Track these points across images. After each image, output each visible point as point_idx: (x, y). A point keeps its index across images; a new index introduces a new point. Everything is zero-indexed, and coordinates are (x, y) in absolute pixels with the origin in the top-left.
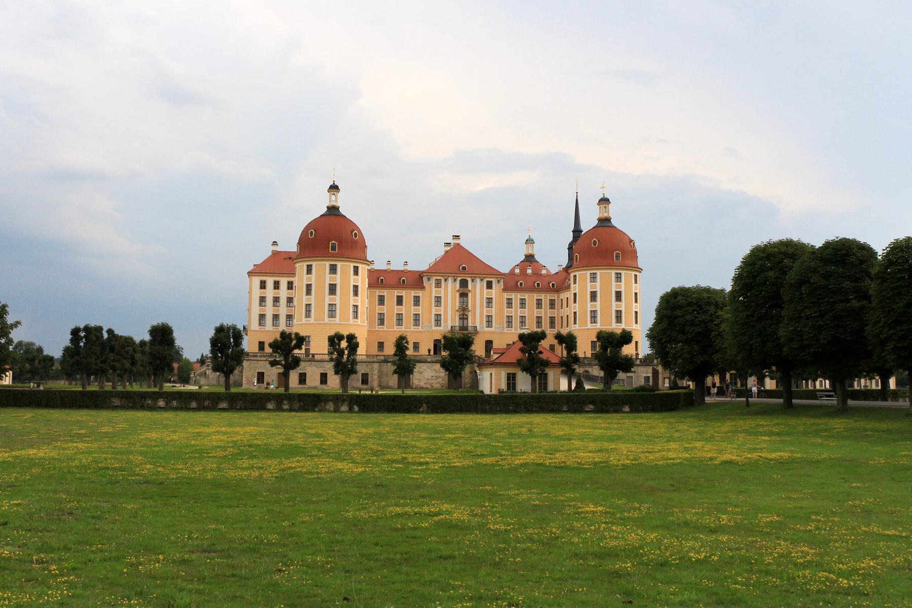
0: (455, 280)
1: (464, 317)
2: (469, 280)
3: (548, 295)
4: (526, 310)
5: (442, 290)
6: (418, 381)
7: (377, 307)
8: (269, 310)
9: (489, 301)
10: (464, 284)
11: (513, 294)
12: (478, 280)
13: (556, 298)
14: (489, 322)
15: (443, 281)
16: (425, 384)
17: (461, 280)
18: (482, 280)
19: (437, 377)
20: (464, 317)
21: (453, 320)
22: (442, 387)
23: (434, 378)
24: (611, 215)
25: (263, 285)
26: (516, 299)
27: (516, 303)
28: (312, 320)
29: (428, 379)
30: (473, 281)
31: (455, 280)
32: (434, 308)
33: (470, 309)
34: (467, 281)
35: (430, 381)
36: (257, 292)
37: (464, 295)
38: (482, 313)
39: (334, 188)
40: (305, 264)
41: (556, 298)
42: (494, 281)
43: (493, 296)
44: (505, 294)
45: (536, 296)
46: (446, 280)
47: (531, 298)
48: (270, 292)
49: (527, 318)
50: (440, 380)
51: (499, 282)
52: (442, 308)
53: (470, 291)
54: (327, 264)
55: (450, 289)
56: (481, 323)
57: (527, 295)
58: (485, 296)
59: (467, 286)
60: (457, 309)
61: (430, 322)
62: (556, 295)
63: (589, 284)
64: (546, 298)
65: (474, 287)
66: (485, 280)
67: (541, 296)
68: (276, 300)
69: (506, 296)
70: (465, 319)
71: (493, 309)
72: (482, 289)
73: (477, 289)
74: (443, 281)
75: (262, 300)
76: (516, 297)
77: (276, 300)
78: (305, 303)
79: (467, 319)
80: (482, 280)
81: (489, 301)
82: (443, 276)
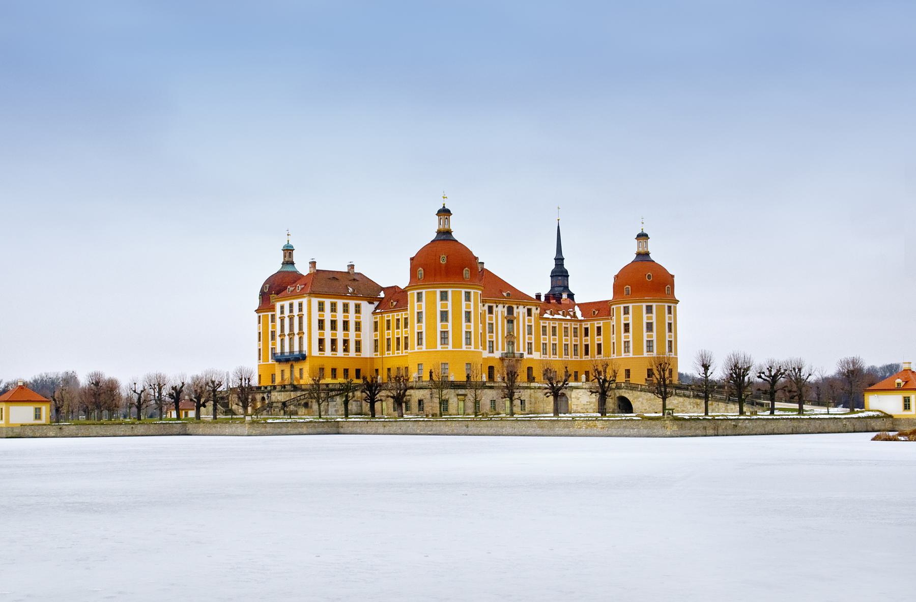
0: (504, 307)
2: (515, 307)
6: (575, 406)
8: (328, 335)
10: (510, 310)
13: (578, 326)
19: (591, 403)
23: (589, 403)
24: (650, 250)
25: (321, 307)
27: (549, 331)
29: (584, 405)
31: (504, 307)
33: (515, 335)
35: (586, 407)
37: (510, 322)
46: (497, 306)
48: (328, 316)
50: (592, 405)
51: (537, 309)
53: (515, 318)
54: (438, 291)
58: (527, 324)
59: (513, 314)
66: (526, 308)
68: (334, 324)
75: (321, 323)
77: (334, 324)
80: (524, 307)
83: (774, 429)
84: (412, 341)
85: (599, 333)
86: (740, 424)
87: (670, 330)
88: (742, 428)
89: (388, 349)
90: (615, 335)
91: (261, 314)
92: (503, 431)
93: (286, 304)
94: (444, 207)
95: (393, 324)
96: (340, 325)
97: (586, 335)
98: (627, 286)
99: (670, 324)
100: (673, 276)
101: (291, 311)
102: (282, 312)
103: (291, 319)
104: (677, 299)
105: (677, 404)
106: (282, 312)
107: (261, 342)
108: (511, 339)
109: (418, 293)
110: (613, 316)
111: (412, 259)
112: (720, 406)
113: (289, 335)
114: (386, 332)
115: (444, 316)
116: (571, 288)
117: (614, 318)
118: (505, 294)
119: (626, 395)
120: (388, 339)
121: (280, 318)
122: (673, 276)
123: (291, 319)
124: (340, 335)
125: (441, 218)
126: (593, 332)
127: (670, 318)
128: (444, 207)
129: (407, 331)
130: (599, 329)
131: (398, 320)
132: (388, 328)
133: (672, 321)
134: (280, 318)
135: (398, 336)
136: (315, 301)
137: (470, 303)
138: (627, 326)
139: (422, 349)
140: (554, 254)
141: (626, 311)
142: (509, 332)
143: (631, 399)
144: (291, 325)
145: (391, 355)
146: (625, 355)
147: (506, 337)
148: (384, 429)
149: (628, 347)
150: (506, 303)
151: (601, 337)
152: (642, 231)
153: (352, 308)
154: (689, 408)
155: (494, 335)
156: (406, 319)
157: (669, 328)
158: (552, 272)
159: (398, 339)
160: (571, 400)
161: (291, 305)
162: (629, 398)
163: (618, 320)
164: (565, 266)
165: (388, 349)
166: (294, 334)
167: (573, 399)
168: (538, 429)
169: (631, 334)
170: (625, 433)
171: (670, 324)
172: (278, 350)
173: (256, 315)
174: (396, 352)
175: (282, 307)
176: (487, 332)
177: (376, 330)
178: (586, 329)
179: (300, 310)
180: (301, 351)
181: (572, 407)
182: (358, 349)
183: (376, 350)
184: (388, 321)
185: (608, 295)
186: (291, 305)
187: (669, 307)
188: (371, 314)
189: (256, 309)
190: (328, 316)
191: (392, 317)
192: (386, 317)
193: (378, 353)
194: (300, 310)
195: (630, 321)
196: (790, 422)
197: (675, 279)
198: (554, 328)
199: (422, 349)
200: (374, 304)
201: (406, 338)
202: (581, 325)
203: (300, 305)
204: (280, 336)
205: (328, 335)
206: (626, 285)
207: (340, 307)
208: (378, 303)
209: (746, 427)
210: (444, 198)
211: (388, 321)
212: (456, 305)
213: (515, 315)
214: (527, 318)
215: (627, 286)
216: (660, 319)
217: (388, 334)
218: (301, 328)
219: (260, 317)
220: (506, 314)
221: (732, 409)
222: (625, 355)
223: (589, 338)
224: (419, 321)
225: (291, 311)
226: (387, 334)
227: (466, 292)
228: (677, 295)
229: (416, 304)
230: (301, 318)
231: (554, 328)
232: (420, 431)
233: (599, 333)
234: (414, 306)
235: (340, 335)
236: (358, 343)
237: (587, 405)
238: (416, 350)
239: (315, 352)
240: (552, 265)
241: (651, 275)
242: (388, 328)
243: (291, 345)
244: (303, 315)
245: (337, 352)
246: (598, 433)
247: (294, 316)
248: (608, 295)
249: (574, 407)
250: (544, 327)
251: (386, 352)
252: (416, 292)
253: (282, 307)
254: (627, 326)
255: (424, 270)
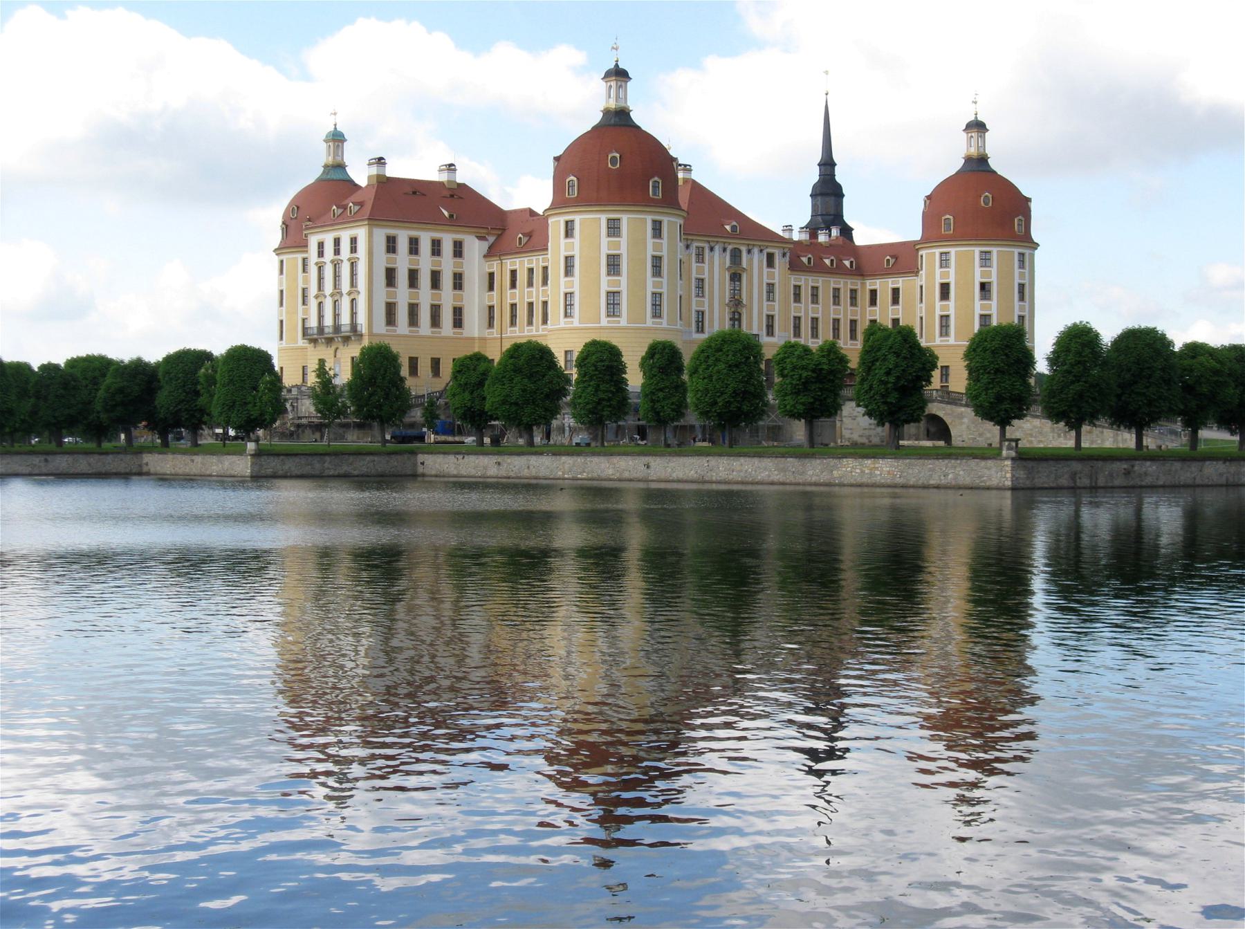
0: (725, 250)
1: (736, 318)
2: (744, 249)
3: (849, 281)
4: (820, 307)
5: (706, 266)
6: (850, 431)
7: (890, 308)
9: (771, 287)
10: (736, 255)
11: (803, 278)
12: (756, 251)
14: (770, 331)
15: (707, 251)
16: (860, 436)
17: (731, 251)
18: (761, 251)
20: (736, 318)
21: (721, 319)
22: (883, 442)
24: (989, 151)
26: (807, 285)
27: (806, 294)
28: (623, 321)
30: (749, 252)
31: (725, 250)
32: (694, 299)
33: (744, 302)
34: (740, 251)
35: (867, 432)
36: (382, 260)
37: (736, 277)
38: (760, 313)
39: (619, 75)
40: (562, 220)
41: (859, 287)
42: (777, 254)
43: (776, 281)
44: (793, 277)
45: (834, 282)
46: (712, 249)
47: (826, 284)
48: (403, 262)
49: (776, 318)
52: (706, 300)
54: (603, 218)
55: (716, 265)
56: (760, 329)
57: (821, 279)
60: (727, 301)
61: (690, 325)
62: (859, 282)
63: (978, 270)
64: (845, 285)
65: (750, 261)
66: (765, 252)
67: (840, 284)
68: (413, 276)
69: (794, 280)
70: (737, 320)
71: (776, 304)
72: (760, 268)
73: (754, 262)
74: (707, 251)
75: (390, 275)
76: (806, 282)
77: (413, 276)
78: (563, 290)
79: (739, 320)
80: (761, 251)
81: (771, 287)
82: (709, 242)
83: (1195, 478)
84: (556, 310)
85: (895, 300)
86: (1136, 468)
87: (1022, 298)
88: (1140, 475)
89: (513, 323)
90: (923, 305)
91: (284, 257)
92: (712, 476)
93: (328, 239)
94: (617, 65)
95: (522, 278)
96: (425, 280)
97: (873, 302)
98: (948, 216)
99: (1022, 287)
100: (1029, 200)
101: (337, 252)
102: (321, 254)
103: (336, 265)
104: (1035, 241)
105: (1031, 430)
106: (321, 254)
107: (284, 308)
108: (736, 306)
109: (567, 222)
110: (922, 269)
111: (557, 159)
112: (1105, 433)
113: (332, 295)
114: (509, 292)
115: (613, 265)
116: (848, 218)
117: (923, 273)
118: (728, 228)
119: (941, 414)
120: (513, 306)
121: (317, 264)
122: (1029, 200)
123: (336, 265)
124: (425, 296)
125: (611, 86)
126: (884, 297)
127: (1022, 276)
128: (617, 65)
129: (547, 290)
130: (896, 292)
131: (531, 271)
132: (513, 285)
133: (1026, 281)
134: (317, 264)
135: (530, 300)
136: (381, 234)
137: (662, 241)
138: (945, 290)
139: (572, 323)
140: (818, 156)
141: (944, 262)
142: (733, 297)
143: (948, 420)
144: (337, 276)
145: (518, 334)
146: (941, 341)
147: (727, 305)
148: (498, 470)
149: (947, 326)
150: (730, 244)
151: (900, 307)
152: (976, 118)
153: (447, 248)
154: (1051, 438)
155: (706, 300)
156: (545, 269)
157: (1019, 292)
158: (815, 187)
159: (531, 305)
160: (841, 421)
161: (337, 242)
162: (944, 419)
163: (931, 275)
164: (838, 179)
165: (513, 323)
166: (341, 294)
167: (844, 419)
168: (776, 472)
169: (951, 303)
170: (932, 482)
171: (1022, 286)
172: (313, 323)
173: (276, 260)
174: (526, 328)
175: (321, 245)
176: (693, 296)
177: (491, 288)
178: (873, 293)
179: (354, 249)
180: (354, 326)
181: (843, 434)
182: (458, 322)
183: (491, 325)
184: (513, 273)
185: (913, 232)
186: (337, 242)
187: (1022, 255)
188: (483, 260)
189: (277, 247)
190: (403, 262)
191: (521, 264)
192: (510, 263)
193: (494, 330)
194: (354, 249)
195: (952, 280)
196: (1224, 466)
197: (1033, 206)
198: (815, 289)
199: (572, 323)
200: (487, 240)
201: (545, 303)
202: (863, 285)
203: (354, 241)
204: (316, 297)
205: (403, 295)
206: (945, 214)
207: (425, 247)
208: (494, 238)
209: (1146, 474)
210: (613, 48)
211: (513, 273)
212: (637, 244)
213: (744, 264)
214: (766, 270)
215: (948, 216)
216: (1005, 275)
217: (513, 296)
218: (353, 283)
219: (282, 262)
220: (728, 263)
221: (1126, 440)
222: (941, 341)
223: (877, 309)
224: (569, 271)
225: (337, 252)
226: (510, 296)
227: (654, 222)
228: (1035, 235)
229: (563, 241)
230: (353, 265)
231: (815, 289)
232: (564, 473)
233: (895, 300)
234: (558, 246)
235: (425, 296)
236: (458, 313)
237: (870, 429)
238: (562, 325)
239: (380, 326)
240: (814, 176)
241: (990, 196)
242: (513, 285)
243: (336, 316)
244: (358, 258)
245: (419, 327)
246: (883, 481)
247: (342, 261)
248: (913, 232)
249: (846, 434)
250: (797, 288)
251: (509, 329)
252: (562, 220)
253: (321, 245)
254: (945, 290)
255: (578, 179)
